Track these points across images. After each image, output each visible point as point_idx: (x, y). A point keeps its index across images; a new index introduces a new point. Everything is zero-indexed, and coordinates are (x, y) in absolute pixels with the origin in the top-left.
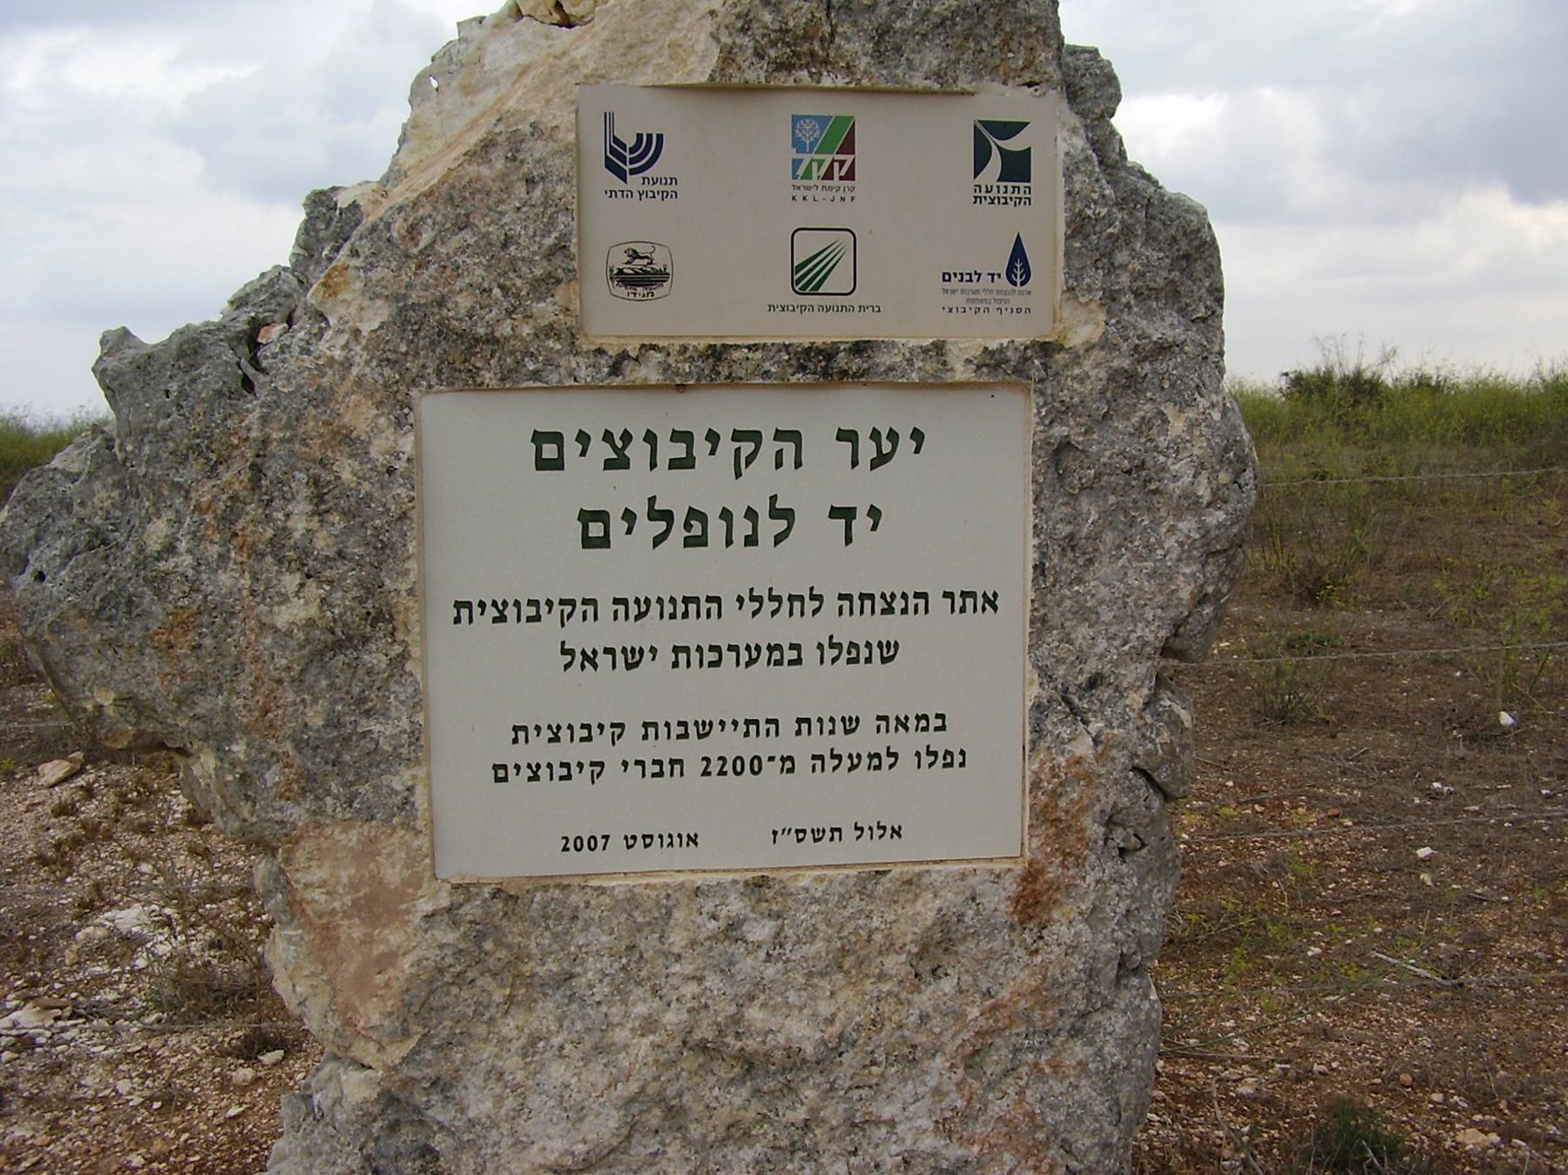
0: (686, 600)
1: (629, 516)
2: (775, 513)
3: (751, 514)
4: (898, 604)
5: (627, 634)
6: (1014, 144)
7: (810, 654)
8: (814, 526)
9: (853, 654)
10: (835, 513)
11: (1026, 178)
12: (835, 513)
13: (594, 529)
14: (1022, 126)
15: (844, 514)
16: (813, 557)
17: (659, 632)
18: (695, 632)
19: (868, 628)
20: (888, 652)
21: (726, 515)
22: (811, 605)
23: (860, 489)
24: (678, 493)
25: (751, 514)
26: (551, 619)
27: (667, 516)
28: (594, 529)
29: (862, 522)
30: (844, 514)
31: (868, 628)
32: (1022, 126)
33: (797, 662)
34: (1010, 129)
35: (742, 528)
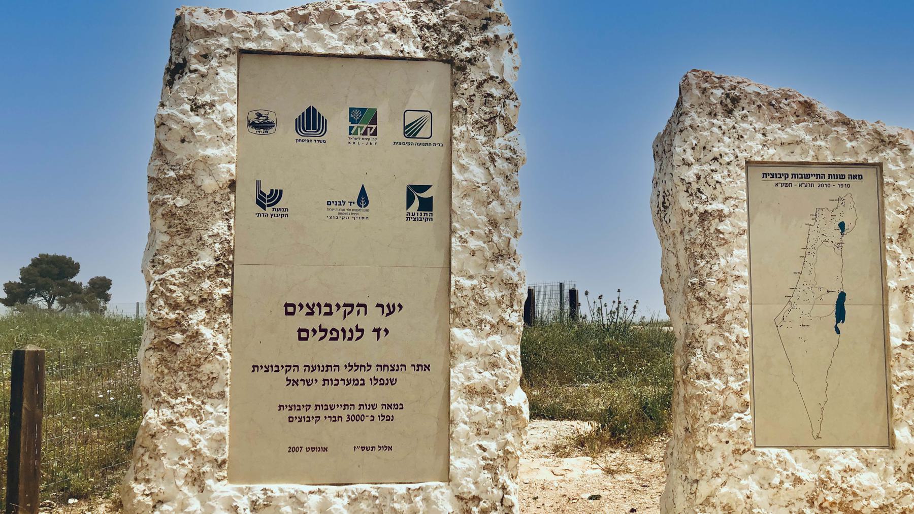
0: (327, 366)
1: (314, 331)
2: (358, 330)
3: (351, 331)
4: (396, 368)
6: (425, 195)
7: (367, 382)
8: (369, 335)
10: (375, 330)
12: (375, 330)
13: (303, 334)
14: (428, 187)
15: (377, 330)
16: (368, 350)
17: (319, 375)
18: (330, 375)
19: (385, 375)
21: (343, 330)
22: (367, 368)
24: (329, 323)
25: (351, 331)
26: (282, 371)
27: (325, 331)
28: (303, 334)
29: (382, 333)
30: (377, 330)
31: (385, 375)
32: (428, 187)
33: (363, 384)
34: (424, 188)
35: (348, 335)
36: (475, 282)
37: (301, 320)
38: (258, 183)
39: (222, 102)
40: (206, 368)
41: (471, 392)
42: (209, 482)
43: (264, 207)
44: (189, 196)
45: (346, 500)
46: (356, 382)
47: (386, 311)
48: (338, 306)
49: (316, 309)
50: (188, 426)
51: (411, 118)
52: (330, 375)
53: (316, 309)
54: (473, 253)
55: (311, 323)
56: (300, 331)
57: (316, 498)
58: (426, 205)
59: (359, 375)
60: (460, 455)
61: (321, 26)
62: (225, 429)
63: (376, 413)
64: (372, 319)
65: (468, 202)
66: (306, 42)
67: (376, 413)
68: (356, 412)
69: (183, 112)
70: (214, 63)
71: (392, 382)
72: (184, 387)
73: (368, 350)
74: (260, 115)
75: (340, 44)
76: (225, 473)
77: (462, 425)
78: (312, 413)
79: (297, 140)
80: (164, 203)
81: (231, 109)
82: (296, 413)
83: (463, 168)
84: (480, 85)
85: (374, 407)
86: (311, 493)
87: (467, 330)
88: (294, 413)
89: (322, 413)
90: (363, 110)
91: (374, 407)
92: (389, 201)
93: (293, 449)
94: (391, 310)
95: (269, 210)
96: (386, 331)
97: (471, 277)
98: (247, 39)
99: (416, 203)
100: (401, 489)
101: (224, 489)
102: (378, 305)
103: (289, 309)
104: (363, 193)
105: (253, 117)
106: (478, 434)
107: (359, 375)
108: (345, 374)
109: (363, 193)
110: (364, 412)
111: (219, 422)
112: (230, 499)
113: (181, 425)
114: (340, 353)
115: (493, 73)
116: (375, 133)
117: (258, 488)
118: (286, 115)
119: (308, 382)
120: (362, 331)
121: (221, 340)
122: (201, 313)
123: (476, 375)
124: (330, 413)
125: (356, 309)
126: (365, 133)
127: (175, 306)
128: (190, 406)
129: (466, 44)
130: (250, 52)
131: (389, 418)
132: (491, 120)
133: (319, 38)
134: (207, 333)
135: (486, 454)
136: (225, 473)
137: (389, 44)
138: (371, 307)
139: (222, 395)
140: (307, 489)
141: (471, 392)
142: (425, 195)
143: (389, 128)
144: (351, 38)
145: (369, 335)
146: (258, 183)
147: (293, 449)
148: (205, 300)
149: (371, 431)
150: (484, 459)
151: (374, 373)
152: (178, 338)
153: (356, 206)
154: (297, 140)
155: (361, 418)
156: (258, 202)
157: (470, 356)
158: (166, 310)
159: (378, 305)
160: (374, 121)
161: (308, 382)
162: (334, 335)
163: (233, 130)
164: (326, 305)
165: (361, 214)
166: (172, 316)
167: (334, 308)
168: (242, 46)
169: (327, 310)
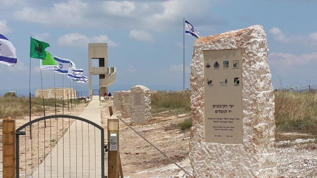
5: (217, 120)
6: (238, 80)
8: (228, 112)
9: (231, 122)
11: (239, 83)
13: (216, 112)
15: (229, 111)
17: (219, 120)
18: (221, 120)
19: (231, 121)
20: (232, 122)
23: (230, 109)
24: (221, 109)
26: (213, 119)
27: (220, 111)
29: (230, 111)
30: (229, 111)
31: (231, 121)
34: (237, 78)
36: (247, 99)
37: (216, 109)
38: (208, 79)
39: (200, 62)
40: (201, 118)
41: (247, 124)
42: (201, 142)
43: (209, 84)
44: (197, 82)
45: (224, 147)
46: (226, 122)
47: (231, 107)
48: (222, 105)
49: (218, 106)
50: (198, 130)
51: (235, 62)
52: (221, 120)
53: (218, 106)
54: (247, 93)
55: (218, 109)
56: (216, 111)
57: (219, 146)
58: (238, 82)
59: (226, 120)
60: (245, 138)
61: (217, 43)
62: (204, 131)
63: (229, 129)
64: (228, 108)
65: (246, 81)
66: (215, 48)
67: (229, 129)
68: (226, 128)
69: (194, 65)
70: (199, 54)
71: (232, 122)
72: (197, 122)
73: (228, 115)
74: (208, 64)
75: (221, 47)
76: (204, 140)
77: (245, 132)
78: (218, 128)
79: (214, 69)
80: (192, 84)
81: (202, 64)
82: (216, 128)
83: (244, 74)
84: (248, 54)
85: (229, 127)
86: (218, 145)
87: (246, 111)
88: (215, 128)
89: (220, 128)
90: (226, 61)
91: (229, 127)
92: (231, 81)
93: (215, 136)
94: (231, 106)
95: (210, 85)
96: (231, 111)
97: (246, 99)
98: (204, 48)
99: (236, 82)
100: (234, 145)
101: (204, 143)
102: (230, 105)
103: (214, 106)
104: (226, 80)
105: (207, 65)
106: (248, 134)
107: (226, 120)
108: (224, 120)
109: (226, 80)
110: (227, 128)
111: (203, 130)
112: (205, 145)
113: (196, 130)
114: (222, 115)
115: (250, 51)
116: (228, 67)
117: (209, 143)
118: (212, 64)
119: (217, 122)
120: (226, 111)
121: (203, 113)
122: (199, 107)
123: (248, 121)
124: (221, 128)
125: (225, 106)
126: (226, 67)
127: (195, 106)
128: (198, 126)
129: (245, 44)
130: (205, 50)
131: (232, 130)
132: (250, 62)
133: (216, 46)
134: (200, 111)
135: (250, 138)
136: (204, 140)
137: (230, 46)
138: (228, 106)
139: (203, 124)
140: (217, 144)
141: (247, 124)
142: (238, 80)
143: (231, 65)
144: (223, 46)
145: (228, 112)
146: (208, 79)
147: (215, 136)
148: (200, 104)
149: (229, 133)
150: (249, 139)
151: (229, 120)
152: (195, 112)
153: (225, 83)
154: (214, 69)
155: (227, 130)
156: (208, 83)
157: (247, 117)
158: (193, 106)
159: (230, 105)
160: (228, 64)
161: (217, 122)
162: (221, 112)
163: (203, 68)
164: (220, 105)
165: (226, 85)
166: (194, 108)
167: (221, 106)
168: (204, 50)
169: (220, 106)
